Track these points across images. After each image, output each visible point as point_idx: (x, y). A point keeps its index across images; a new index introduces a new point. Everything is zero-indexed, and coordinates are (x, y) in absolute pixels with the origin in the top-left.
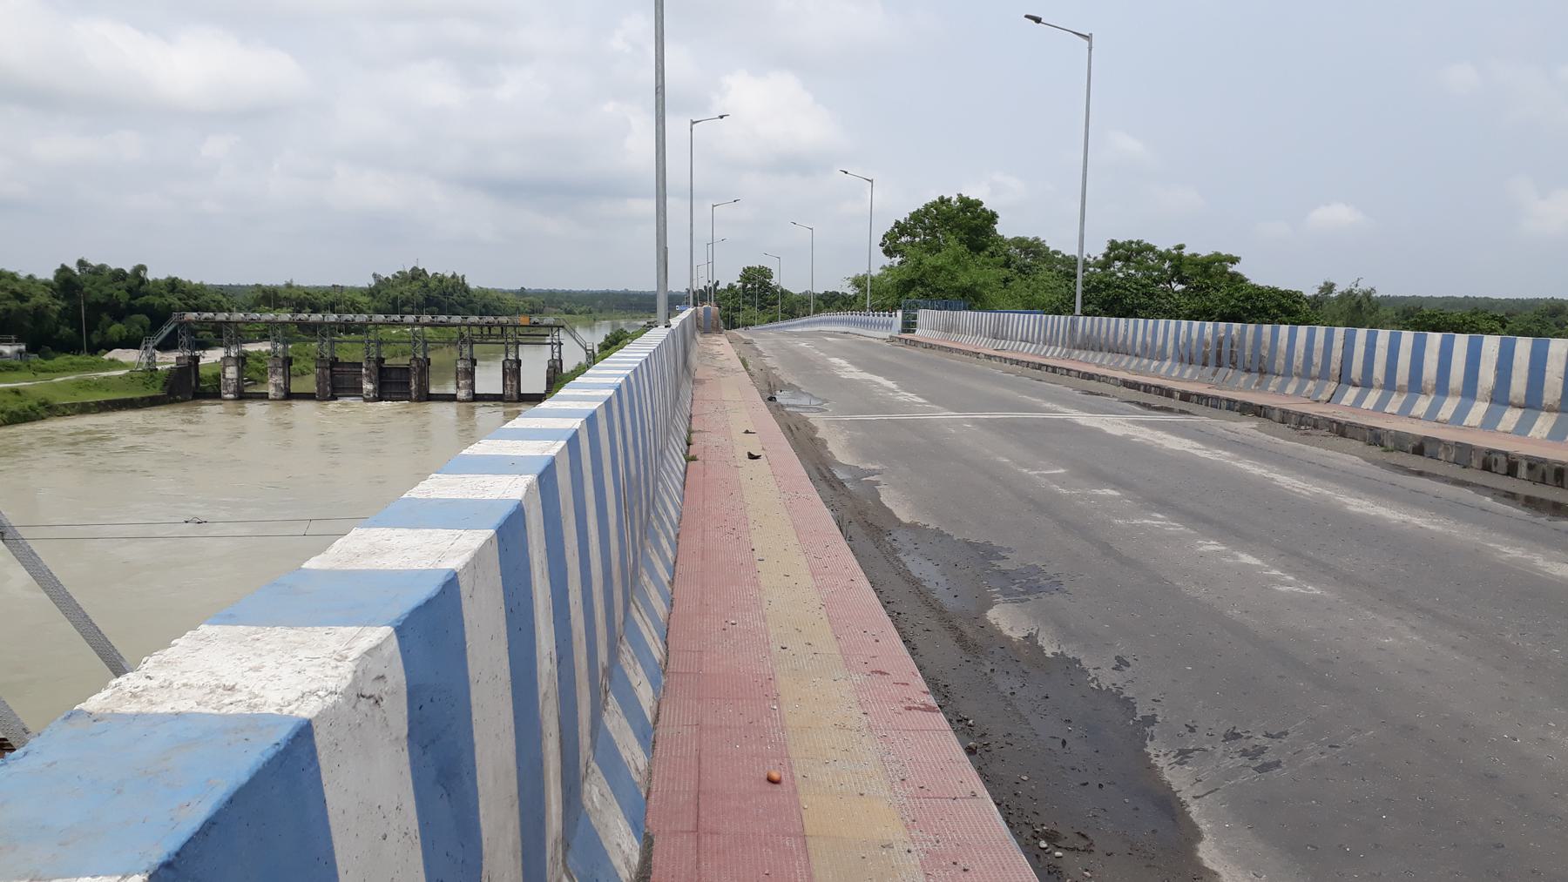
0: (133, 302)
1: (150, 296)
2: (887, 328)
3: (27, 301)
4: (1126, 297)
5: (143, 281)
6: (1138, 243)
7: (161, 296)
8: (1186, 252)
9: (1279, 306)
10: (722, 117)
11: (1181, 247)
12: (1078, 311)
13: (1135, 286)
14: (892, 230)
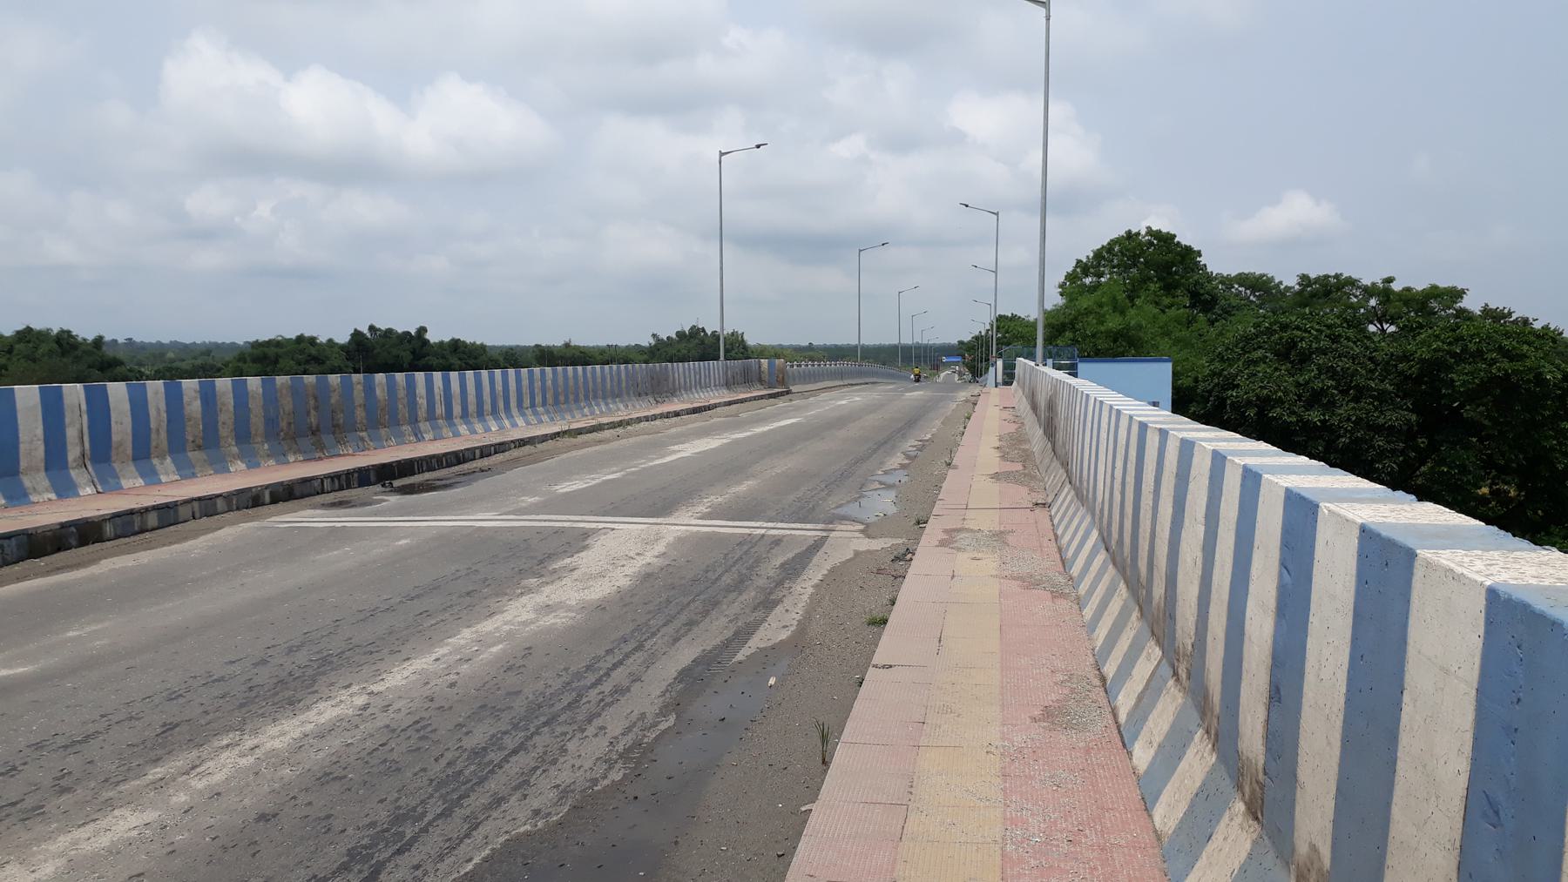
0: (416, 363)
1: (430, 357)
2: (805, 379)
4: (1302, 339)
5: (426, 342)
6: (1337, 276)
7: (443, 357)
8: (1396, 287)
9: (1501, 349)
10: (758, 147)
11: (1390, 280)
12: (722, 358)
13: (1317, 327)
14: (1074, 271)
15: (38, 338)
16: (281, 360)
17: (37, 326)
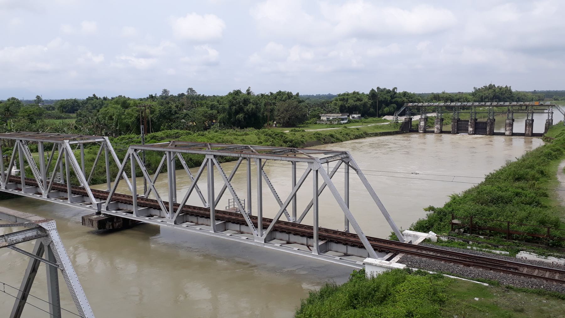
0: (392, 100)
3: (362, 101)
5: (395, 93)
7: (401, 98)
15: (282, 94)
16: (349, 100)
17: (282, 91)
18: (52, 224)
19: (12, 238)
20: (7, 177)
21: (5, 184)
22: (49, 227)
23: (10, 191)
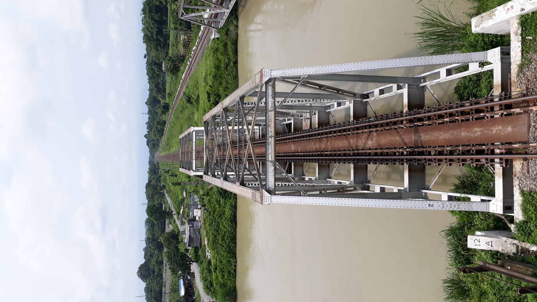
18: (266, 72)
19: (269, 106)
20: (217, 6)
21: (223, 9)
22: (267, 75)
23: (231, 6)
